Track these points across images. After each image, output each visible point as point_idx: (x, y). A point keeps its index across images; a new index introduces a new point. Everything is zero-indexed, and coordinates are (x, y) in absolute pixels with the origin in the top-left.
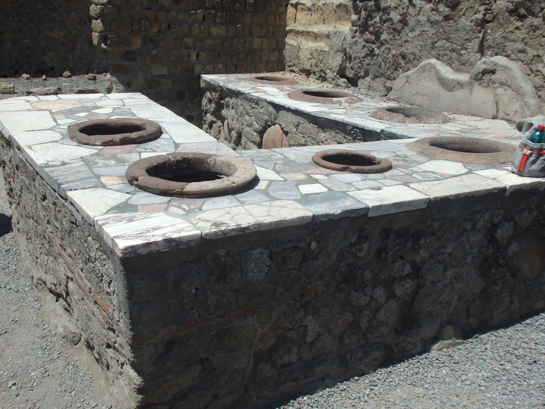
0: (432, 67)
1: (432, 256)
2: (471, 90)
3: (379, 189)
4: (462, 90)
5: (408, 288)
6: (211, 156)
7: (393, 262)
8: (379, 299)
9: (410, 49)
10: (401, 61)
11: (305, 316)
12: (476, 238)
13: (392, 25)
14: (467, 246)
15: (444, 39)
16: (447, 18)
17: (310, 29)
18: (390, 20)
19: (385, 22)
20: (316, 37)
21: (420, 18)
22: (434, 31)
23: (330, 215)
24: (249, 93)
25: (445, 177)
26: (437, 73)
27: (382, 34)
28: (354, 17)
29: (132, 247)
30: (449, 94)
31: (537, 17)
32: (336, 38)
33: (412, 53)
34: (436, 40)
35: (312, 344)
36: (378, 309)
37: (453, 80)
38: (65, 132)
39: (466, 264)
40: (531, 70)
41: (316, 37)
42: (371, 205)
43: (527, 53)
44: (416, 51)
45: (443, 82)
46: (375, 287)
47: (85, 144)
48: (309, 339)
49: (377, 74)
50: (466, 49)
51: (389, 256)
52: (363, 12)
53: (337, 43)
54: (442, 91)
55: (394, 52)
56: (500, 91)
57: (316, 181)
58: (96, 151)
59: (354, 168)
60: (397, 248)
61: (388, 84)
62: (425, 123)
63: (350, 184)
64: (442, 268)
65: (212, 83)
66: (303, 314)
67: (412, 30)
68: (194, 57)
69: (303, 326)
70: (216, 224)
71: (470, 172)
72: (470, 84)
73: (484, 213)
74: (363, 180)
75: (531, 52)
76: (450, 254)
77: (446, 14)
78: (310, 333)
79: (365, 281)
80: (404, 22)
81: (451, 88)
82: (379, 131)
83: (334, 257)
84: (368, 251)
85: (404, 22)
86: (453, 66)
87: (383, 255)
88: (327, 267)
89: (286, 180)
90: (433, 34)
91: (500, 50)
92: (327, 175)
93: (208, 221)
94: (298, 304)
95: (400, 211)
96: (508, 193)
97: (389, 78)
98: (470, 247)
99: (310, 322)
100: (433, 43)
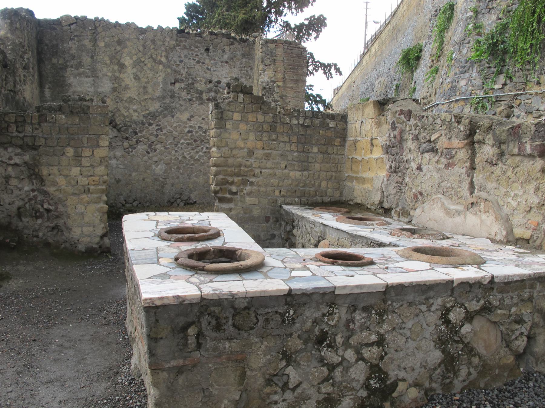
1: (394, 329)
3: (353, 276)
4: (459, 217)
5: (374, 353)
6: (239, 249)
7: (361, 331)
8: (349, 359)
10: (419, 196)
11: (287, 365)
12: (433, 318)
14: (425, 325)
23: (303, 290)
25: (409, 271)
26: (443, 204)
29: (151, 299)
30: (451, 220)
35: (294, 390)
36: (350, 367)
38: (157, 232)
39: (425, 338)
42: (337, 285)
46: (346, 349)
47: (165, 240)
48: (291, 386)
51: (356, 326)
54: (447, 218)
57: (308, 269)
58: (169, 244)
59: (340, 262)
60: (363, 320)
62: (426, 239)
63: (332, 272)
64: (404, 340)
65: (288, 211)
66: (285, 364)
68: (277, 193)
69: (286, 374)
70: (215, 290)
71: (432, 269)
73: (437, 299)
74: (344, 270)
76: (410, 329)
78: (292, 380)
79: (337, 344)
81: (452, 215)
83: (309, 324)
84: (338, 321)
86: (453, 199)
87: (351, 326)
88: (304, 330)
89: (286, 267)
92: (319, 266)
93: (211, 288)
94: (281, 356)
95: (362, 291)
96: (455, 285)
98: (427, 325)
99: (290, 370)
100: (439, 184)
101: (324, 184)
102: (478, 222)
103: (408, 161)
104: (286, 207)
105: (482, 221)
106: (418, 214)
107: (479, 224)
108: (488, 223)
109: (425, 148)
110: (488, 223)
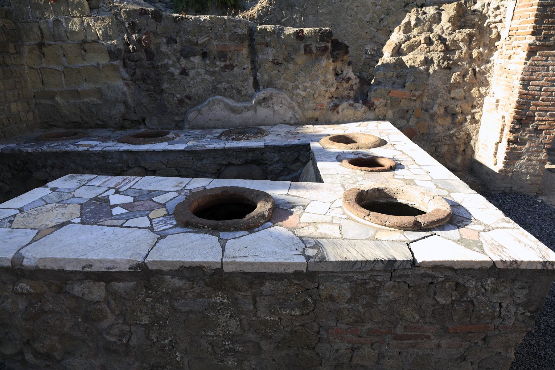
2: (256, 112)
10: (187, 100)
22: (214, 78)
24: (86, 150)
26: (226, 105)
45: (233, 110)
54: (232, 115)
55: (178, 96)
80: (184, 72)
82: (263, 147)
85: (184, 72)
86: (235, 98)
91: (270, 84)
101: (13, 106)
102: (272, 112)
103: (166, 66)
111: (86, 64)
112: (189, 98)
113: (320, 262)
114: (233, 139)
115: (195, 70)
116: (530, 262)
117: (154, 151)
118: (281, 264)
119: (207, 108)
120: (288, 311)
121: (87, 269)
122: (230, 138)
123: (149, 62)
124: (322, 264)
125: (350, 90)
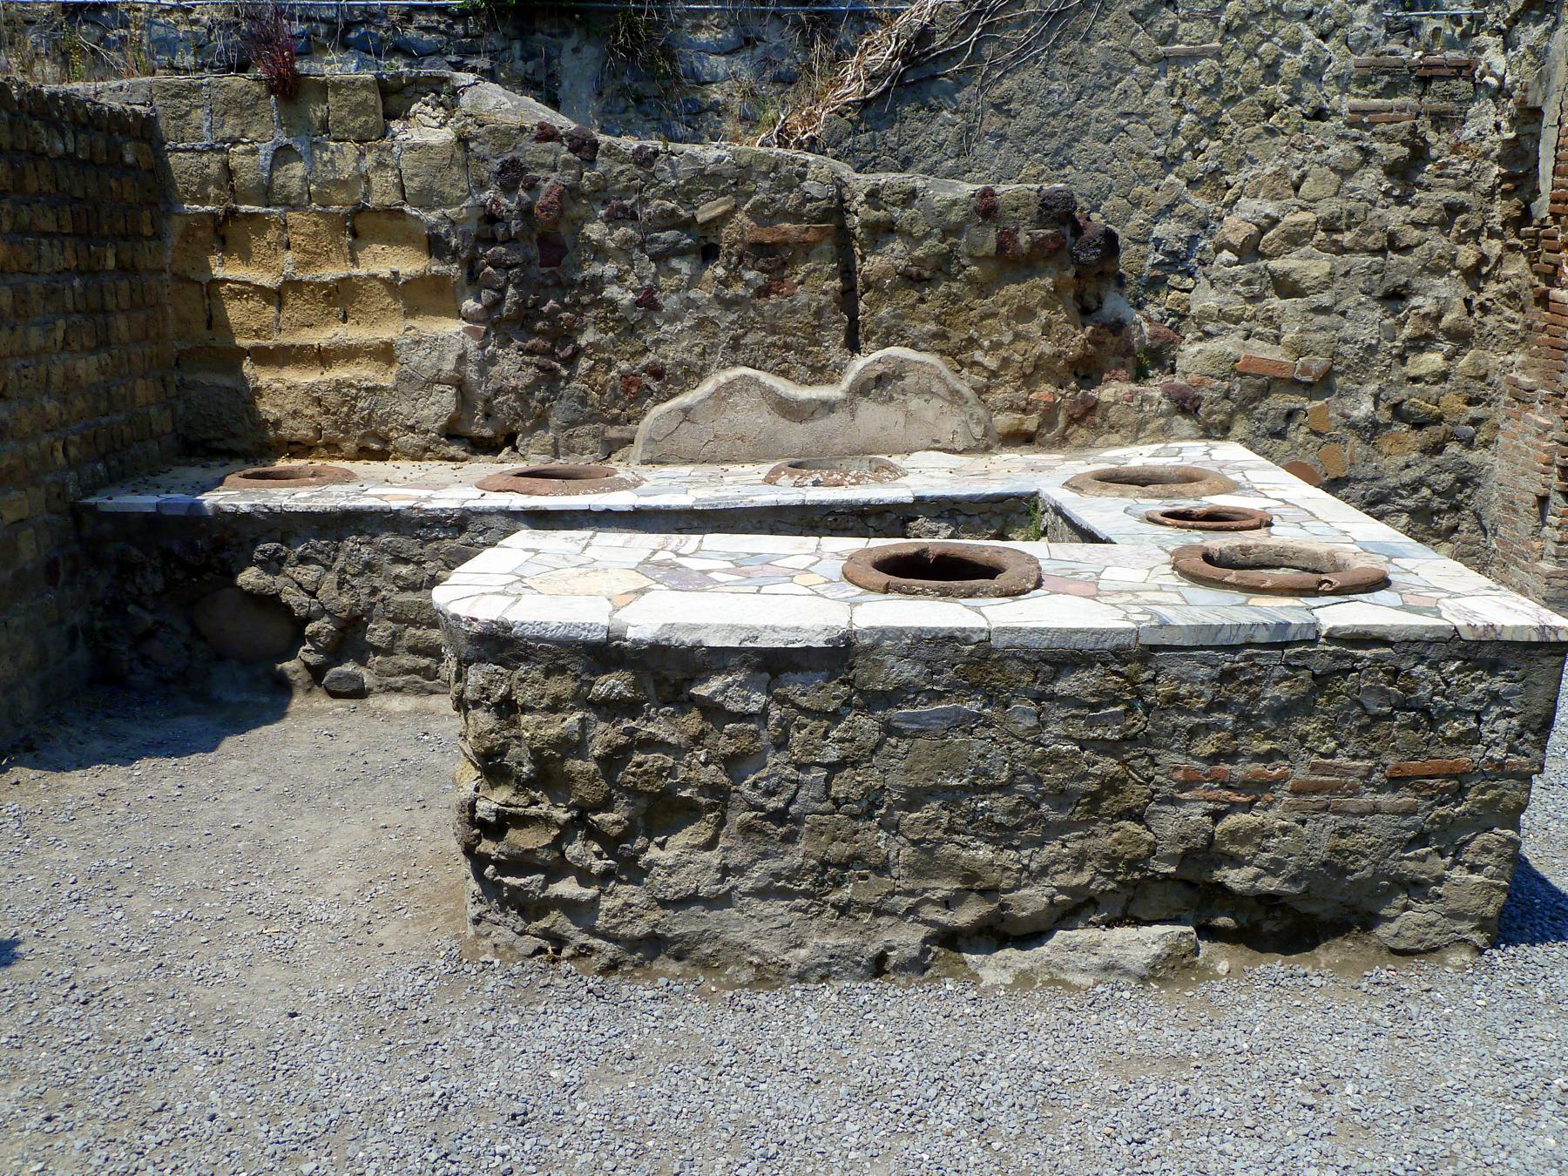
0: (756, 382)
9: (670, 355)
10: (648, 380)
13: (615, 310)
15: (761, 329)
16: (763, 292)
17: (286, 340)
18: (612, 304)
19: (585, 307)
20: (322, 357)
21: (692, 294)
22: (733, 317)
26: (767, 393)
27: (581, 331)
28: (469, 304)
30: (800, 427)
31: (955, 280)
32: (422, 353)
33: (679, 364)
34: (740, 331)
37: (810, 401)
40: (960, 363)
41: (322, 357)
43: (948, 338)
44: (694, 359)
49: (576, 416)
50: (818, 343)
52: (511, 291)
53: (427, 363)
54: (783, 423)
55: (624, 366)
56: (915, 403)
61: (613, 432)
67: (674, 318)
72: (849, 403)
75: (957, 337)
77: (761, 283)
80: (648, 302)
82: (911, 500)
85: (648, 302)
86: (794, 374)
90: (733, 323)
97: (615, 421)
100: (736, 339)
103: (597, 283)
104: (99, 500)
105: (908, 415)
106: (664, 431)
107: (902, 420)
108: (930, 415)
109: (677, 243)
110: (930, 415)
111: (355, 271)
112: (657, 373)
113: (1161, 626)
114: (816, 484)
115: (682, 294)
116: (1516, 628)
117: (608, 511)
118: (1094, 632)
119: (711, 402)
120: (1099, 731)
121: (748, 644)
122: (809, 481)
123: (546, 270)
124: (1163, 632)
125: (1124, 356)
